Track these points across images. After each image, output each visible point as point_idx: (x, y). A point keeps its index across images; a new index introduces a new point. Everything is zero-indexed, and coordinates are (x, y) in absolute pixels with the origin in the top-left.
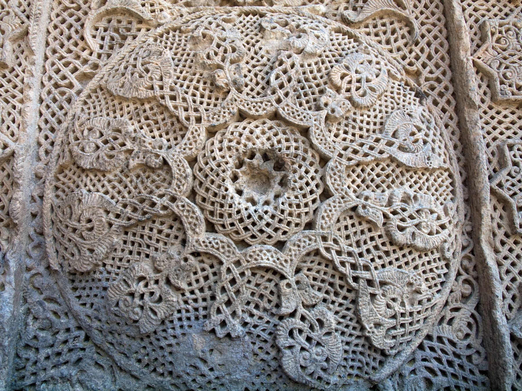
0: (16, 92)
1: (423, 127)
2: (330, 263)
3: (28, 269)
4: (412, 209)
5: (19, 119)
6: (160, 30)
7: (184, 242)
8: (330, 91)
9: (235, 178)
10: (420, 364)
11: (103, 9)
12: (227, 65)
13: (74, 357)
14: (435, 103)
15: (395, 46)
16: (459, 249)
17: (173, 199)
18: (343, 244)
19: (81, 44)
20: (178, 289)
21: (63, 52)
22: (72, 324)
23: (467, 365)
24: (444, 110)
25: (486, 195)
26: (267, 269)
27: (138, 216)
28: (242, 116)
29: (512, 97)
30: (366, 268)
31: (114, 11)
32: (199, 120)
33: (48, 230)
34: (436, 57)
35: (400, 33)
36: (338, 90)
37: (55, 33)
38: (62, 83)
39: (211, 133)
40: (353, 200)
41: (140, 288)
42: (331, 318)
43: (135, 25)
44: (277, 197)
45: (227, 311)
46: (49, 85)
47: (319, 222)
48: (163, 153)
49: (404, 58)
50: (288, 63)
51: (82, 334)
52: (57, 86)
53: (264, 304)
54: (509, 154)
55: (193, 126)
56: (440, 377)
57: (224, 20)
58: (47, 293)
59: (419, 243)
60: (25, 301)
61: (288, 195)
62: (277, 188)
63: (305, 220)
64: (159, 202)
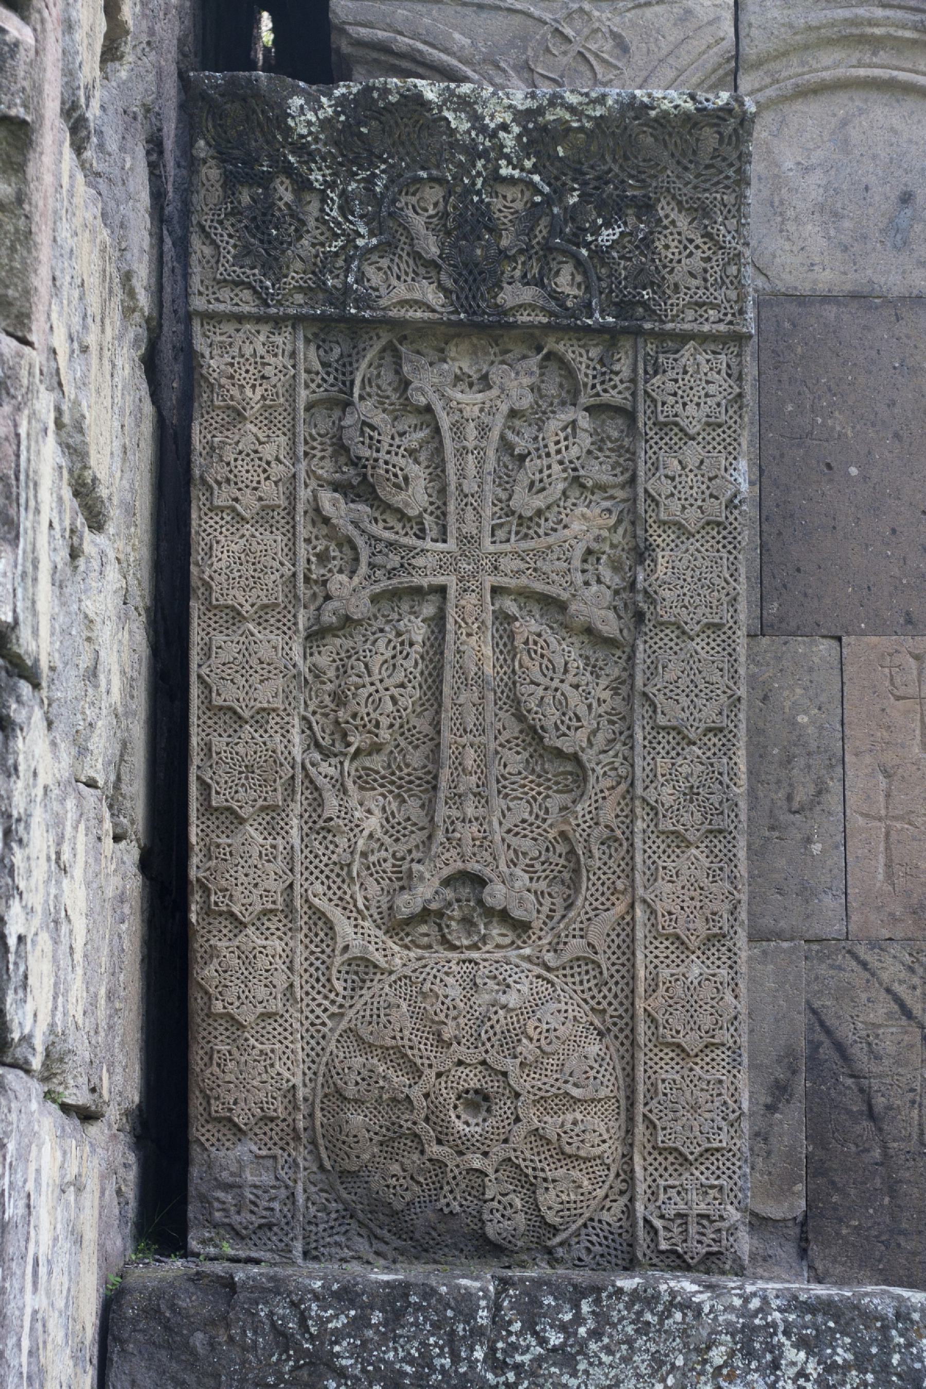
0: (287, 1034)
1: (596, 1066)
2: (518, 1166)
3: (305, 1169)
4: (577, 1130)
5: (292, 1056)
6: (393, 977)
7: (422, 1152)
8: (524, 1041)
9: (455, 1107)
10: (583, 1237)
11: (346, 956)
12: (450, 1022)
13: (343, 1229)
14: (616, 1037)
15: (586, 985)
16: (619, 1157)
17: (415, 1123)
18: (528, 1154)
19: (328, 986)
20: (418, 1183)
21: (314, 993)
22: (341, 1207)
23: (619, 1240)
24: (622, 1044)
25: (639, 1119)
26: (477, 1170)
27: (390, 1134)
28: (460, 1063)
29: (670, 1040)
30: (543, 1170)
31: (355, 958)
32: (430, 1066)
33: (321, 1141)
34: (621, 995)
35: (592, 973)
36: (531, 1039)
37: (306, 976)
38: (318, 1021)
39: (439, 1075)
40: (536, 1123)
41: (393, 1181)
42: (518, 1203)
43: (372, 970)
44: (484, 1120)
45: (450, 1196)
46: (307, 1024)
47: (512, 1139)
48: (406, 1090)
49: (593, 997)
50: (495, 1018)
51: (348, 1214)
52: (312, 1024)
53: (474, 1192)
54: (661, 1086)
55: (427, 1071)
56: (598, 1247)
57: (447, 974)
58: (320, 1186)
59: (582, 1153)
60: (305, 1191)
61: (491, 1121)
62: (484, 1114)
63: (503, 1137)
64: (405, 1125)
